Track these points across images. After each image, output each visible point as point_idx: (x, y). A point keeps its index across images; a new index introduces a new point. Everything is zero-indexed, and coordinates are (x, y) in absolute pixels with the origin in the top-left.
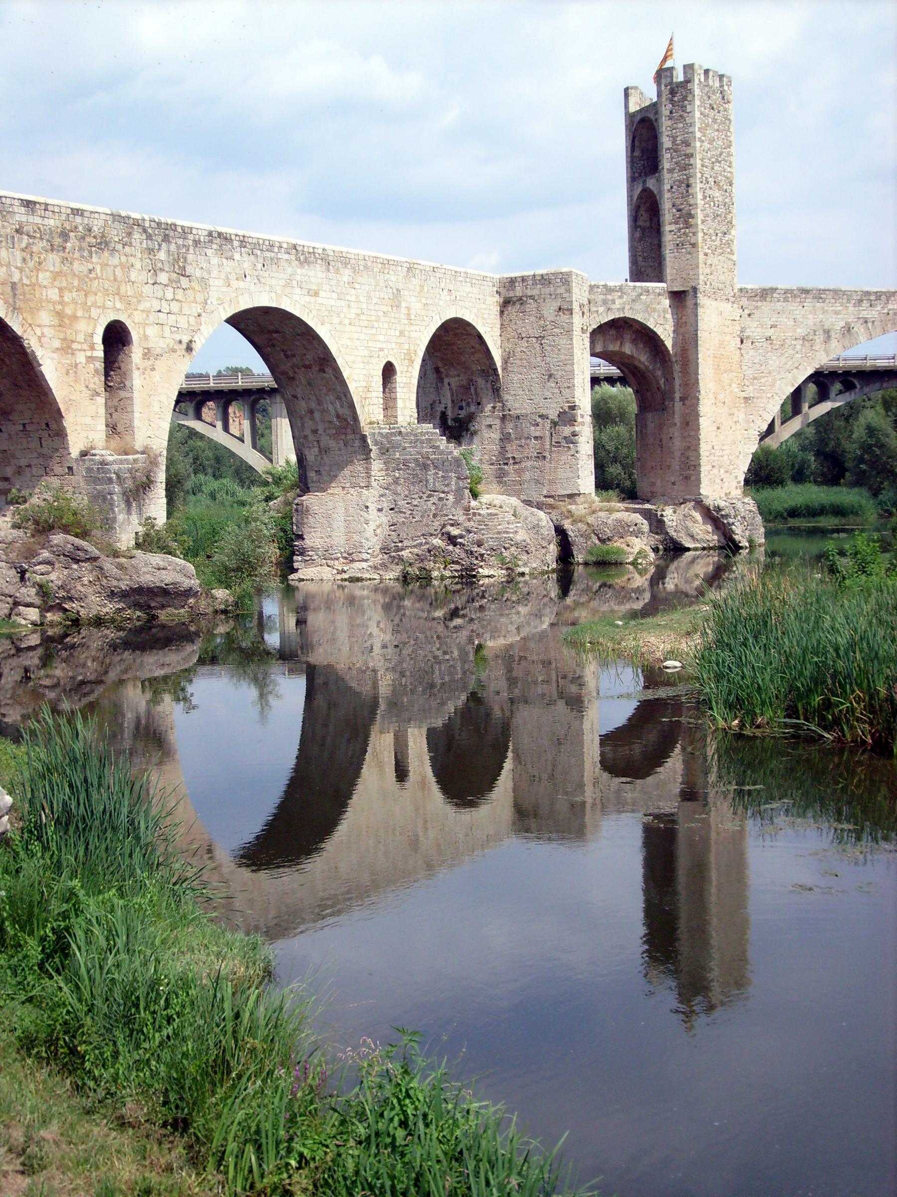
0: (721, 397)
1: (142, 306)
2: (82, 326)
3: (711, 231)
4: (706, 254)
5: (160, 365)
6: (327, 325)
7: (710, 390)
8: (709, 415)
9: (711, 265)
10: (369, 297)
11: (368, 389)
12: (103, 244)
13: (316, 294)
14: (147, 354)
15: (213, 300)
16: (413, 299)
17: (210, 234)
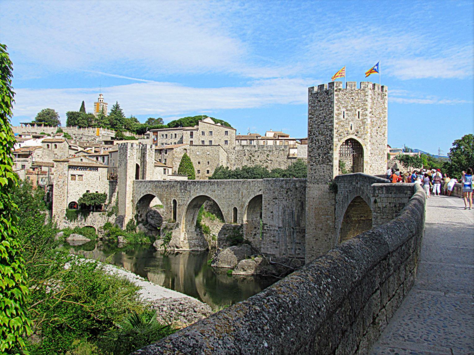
0: (320, 226)
1: (179, 196)
2: (169, 201)
3: (317, 155)
4: (312, 165)
5: (181, 207)
6: (217, 199)
7: (312, 223)
8: (311, 233)
9: (315, 169)
10: (229, 191)
11: (228, 214)
12: (173, 186)
13: (214, 192)
14: (179, 205)
15: (191, 195)
16: (244, 190)
17: (192, 181)
